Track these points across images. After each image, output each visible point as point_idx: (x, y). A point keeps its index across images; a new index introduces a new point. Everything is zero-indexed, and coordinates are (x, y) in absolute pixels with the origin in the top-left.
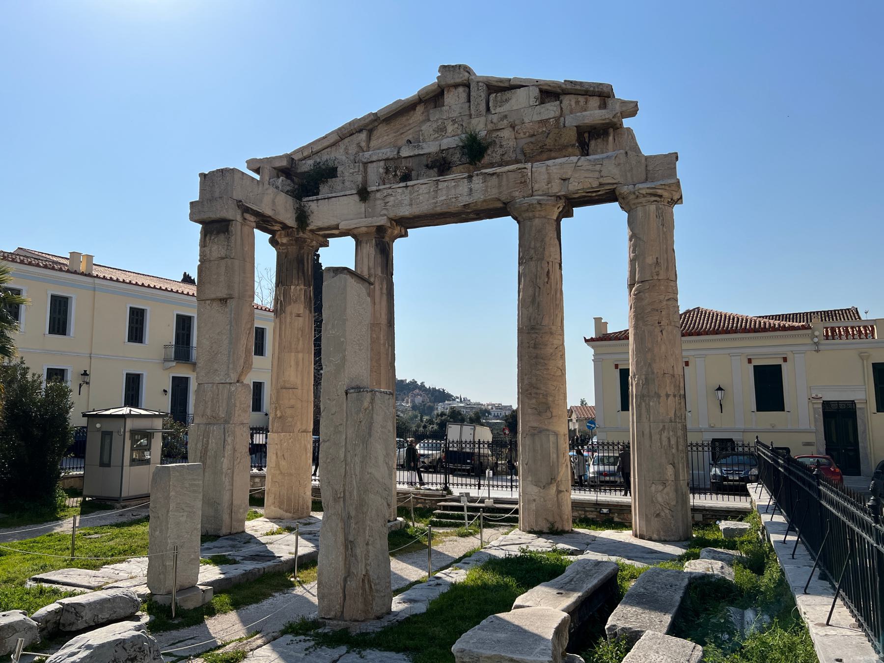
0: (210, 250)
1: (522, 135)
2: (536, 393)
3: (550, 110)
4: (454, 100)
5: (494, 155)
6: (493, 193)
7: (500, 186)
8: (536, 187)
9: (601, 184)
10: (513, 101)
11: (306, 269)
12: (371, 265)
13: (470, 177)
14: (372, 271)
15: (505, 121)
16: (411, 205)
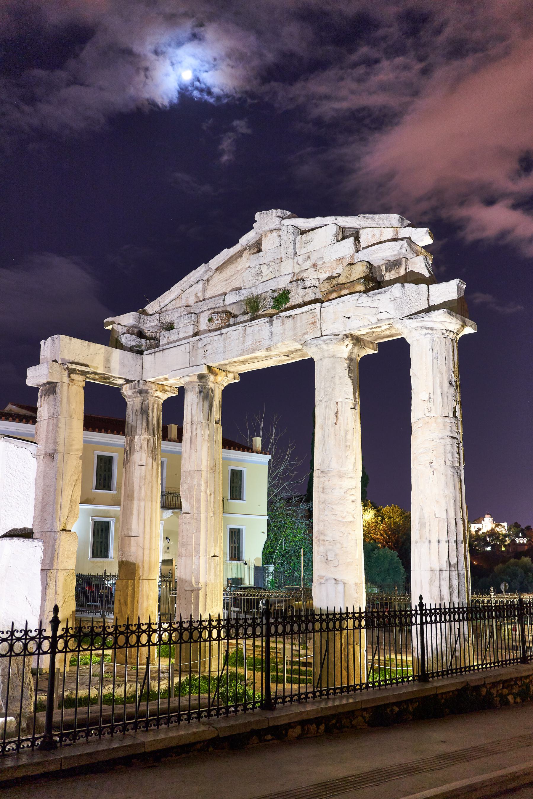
2: (324, 540)
5: (297, 296)
7: (295, 328)
11: (150, 419)
13: (271, 322)
15: (308, 261)
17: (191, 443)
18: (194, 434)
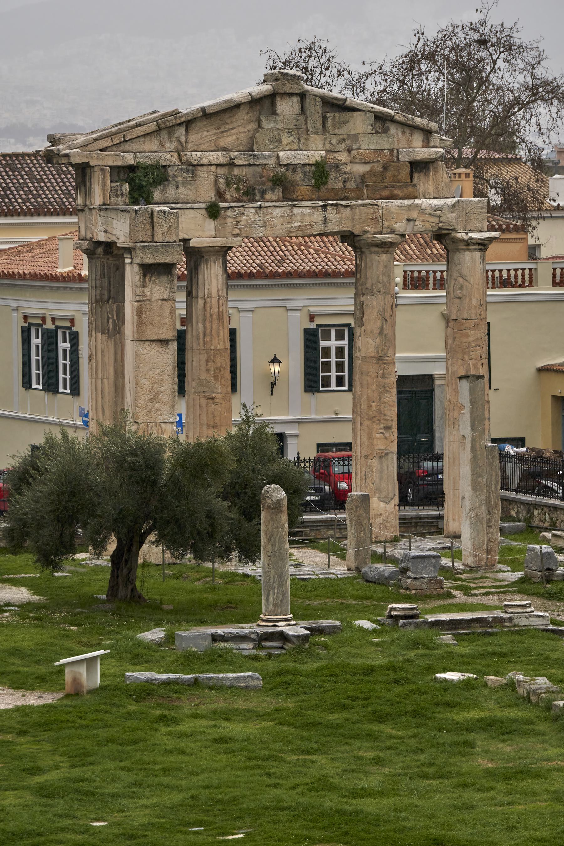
0: (151, 291)
1: (357, 161)
4: (287, 108)
6: (346, 227)
8: (386, 224)
9: (440, 229)
10: (351, 124)
12: (220, 286)
13: (324, 207)
14: (220, 292)
15: (343, 144)
16: (264, 226)
17: (219, 319)
18: (221, 310)
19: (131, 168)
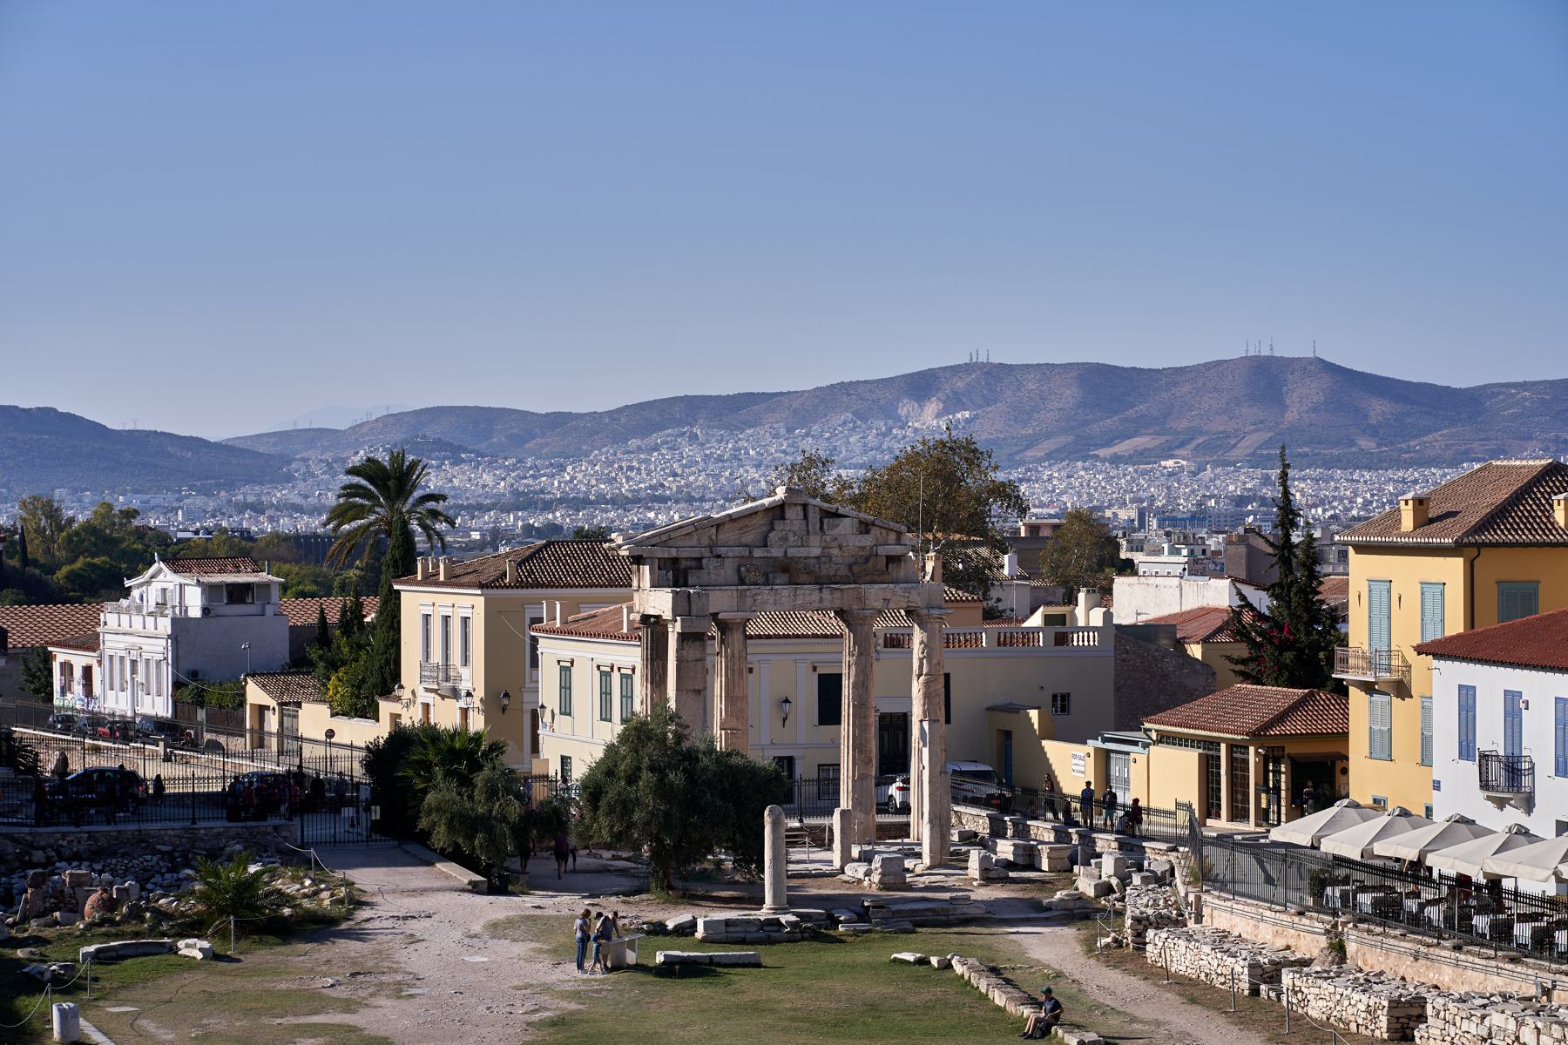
3: (867, 541)
4: (793, 514)
6: (838, 604)
19: (675, 560)
